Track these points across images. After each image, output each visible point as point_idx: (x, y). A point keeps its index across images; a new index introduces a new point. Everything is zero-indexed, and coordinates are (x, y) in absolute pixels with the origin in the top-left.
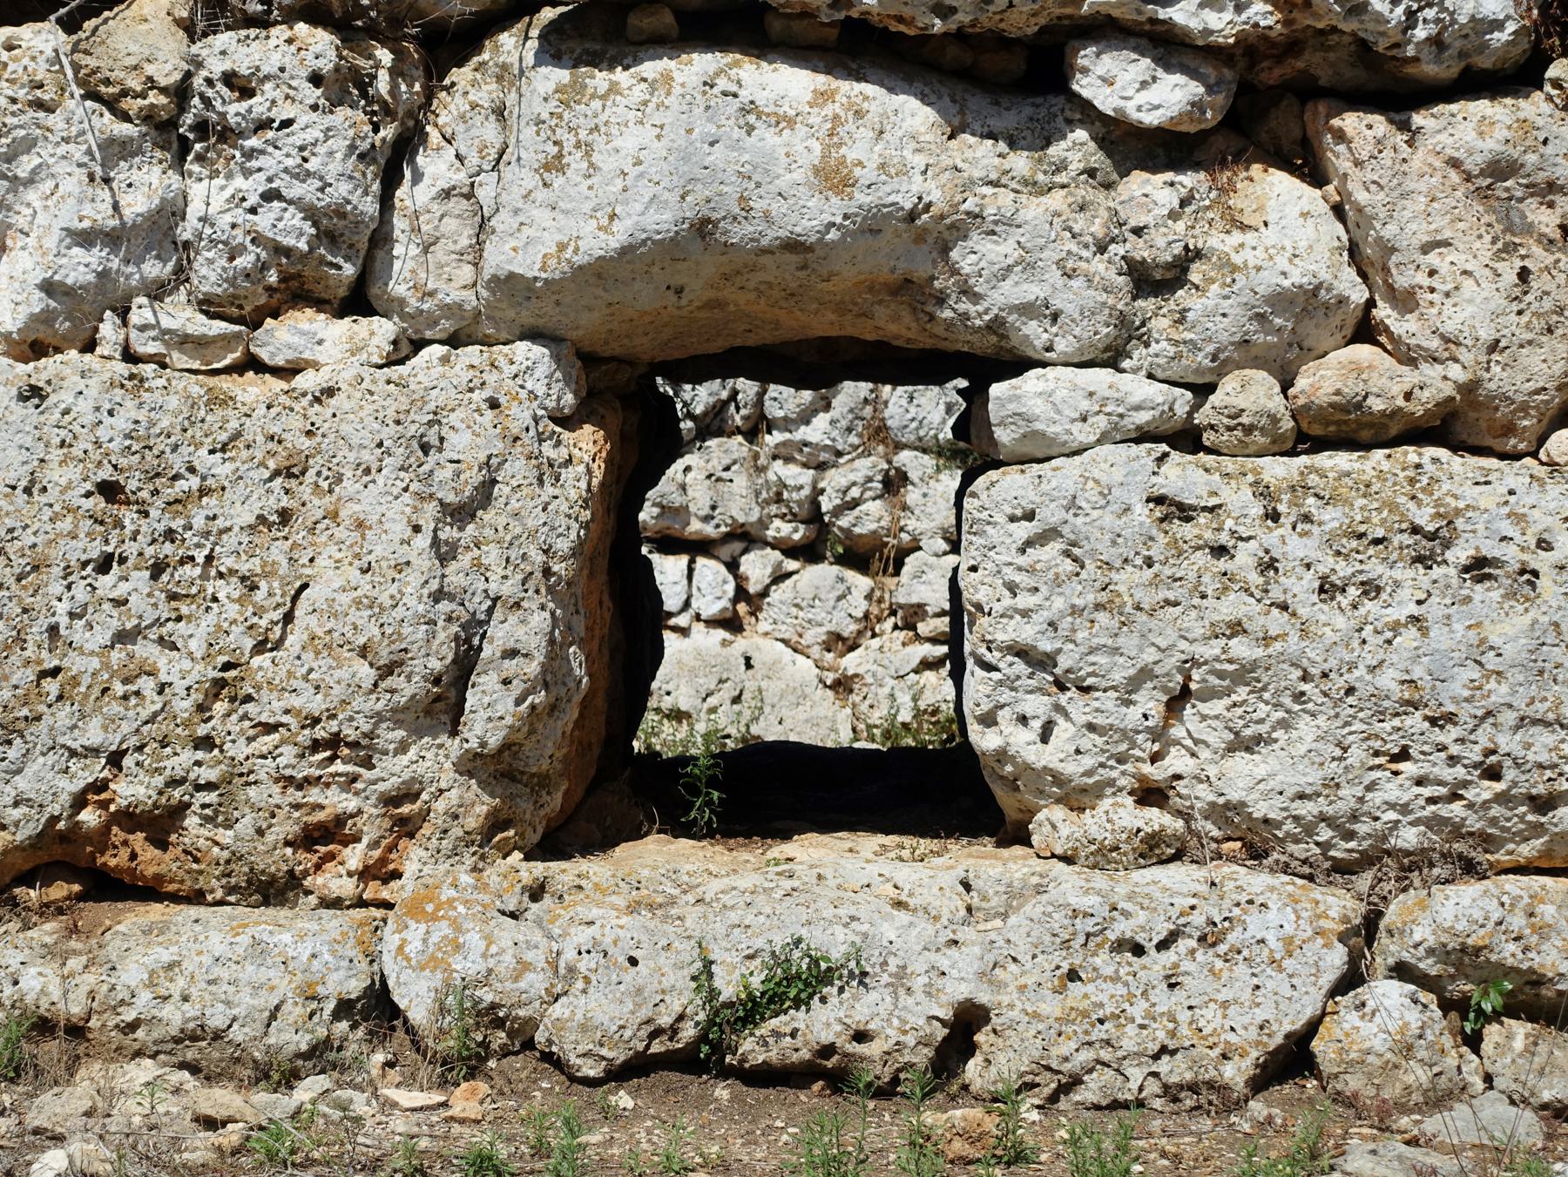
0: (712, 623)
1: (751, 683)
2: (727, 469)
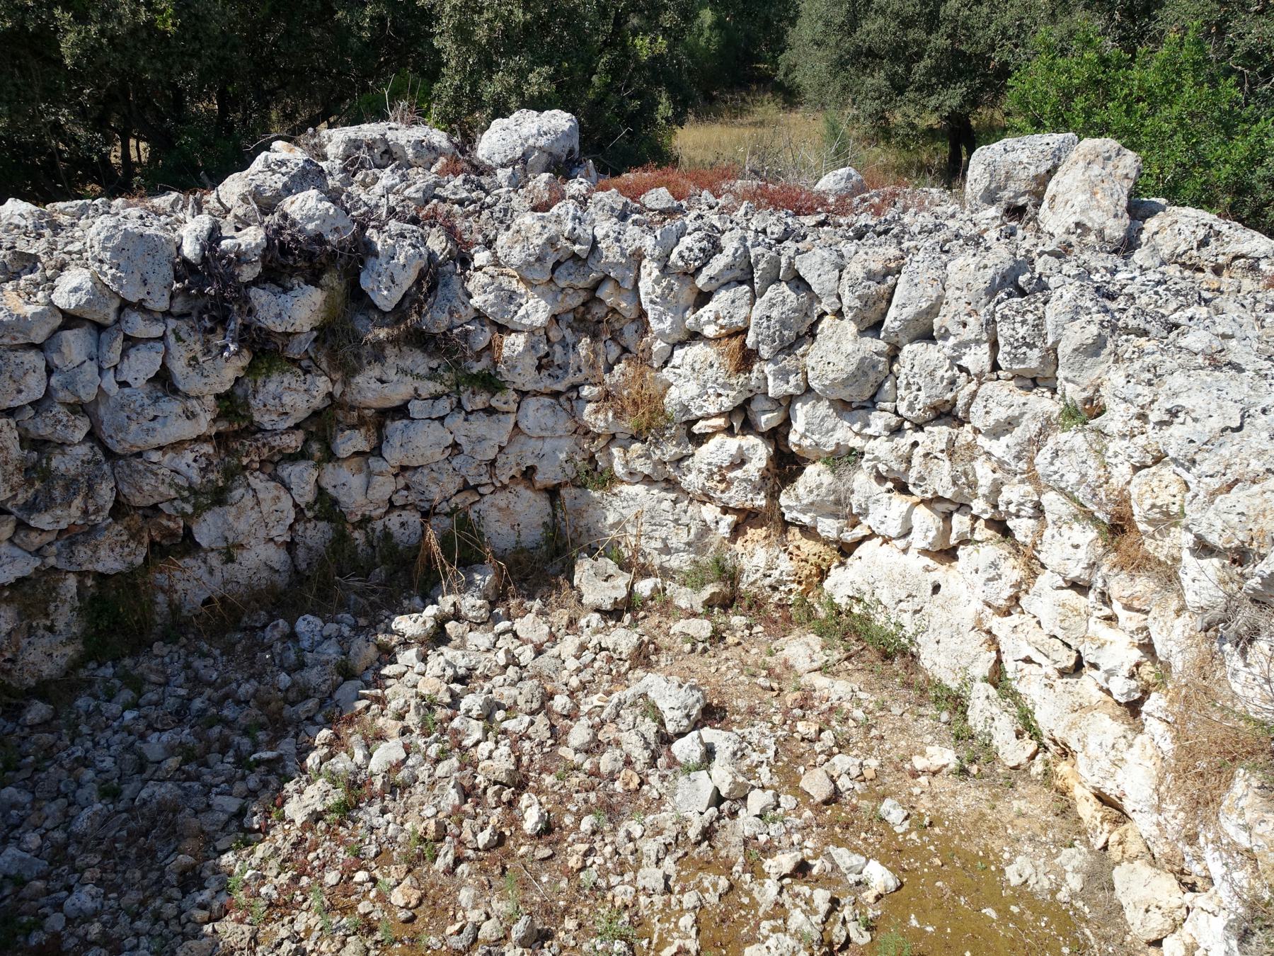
0: (925, 552)
1: (932, 606)
2: (942, 451)
